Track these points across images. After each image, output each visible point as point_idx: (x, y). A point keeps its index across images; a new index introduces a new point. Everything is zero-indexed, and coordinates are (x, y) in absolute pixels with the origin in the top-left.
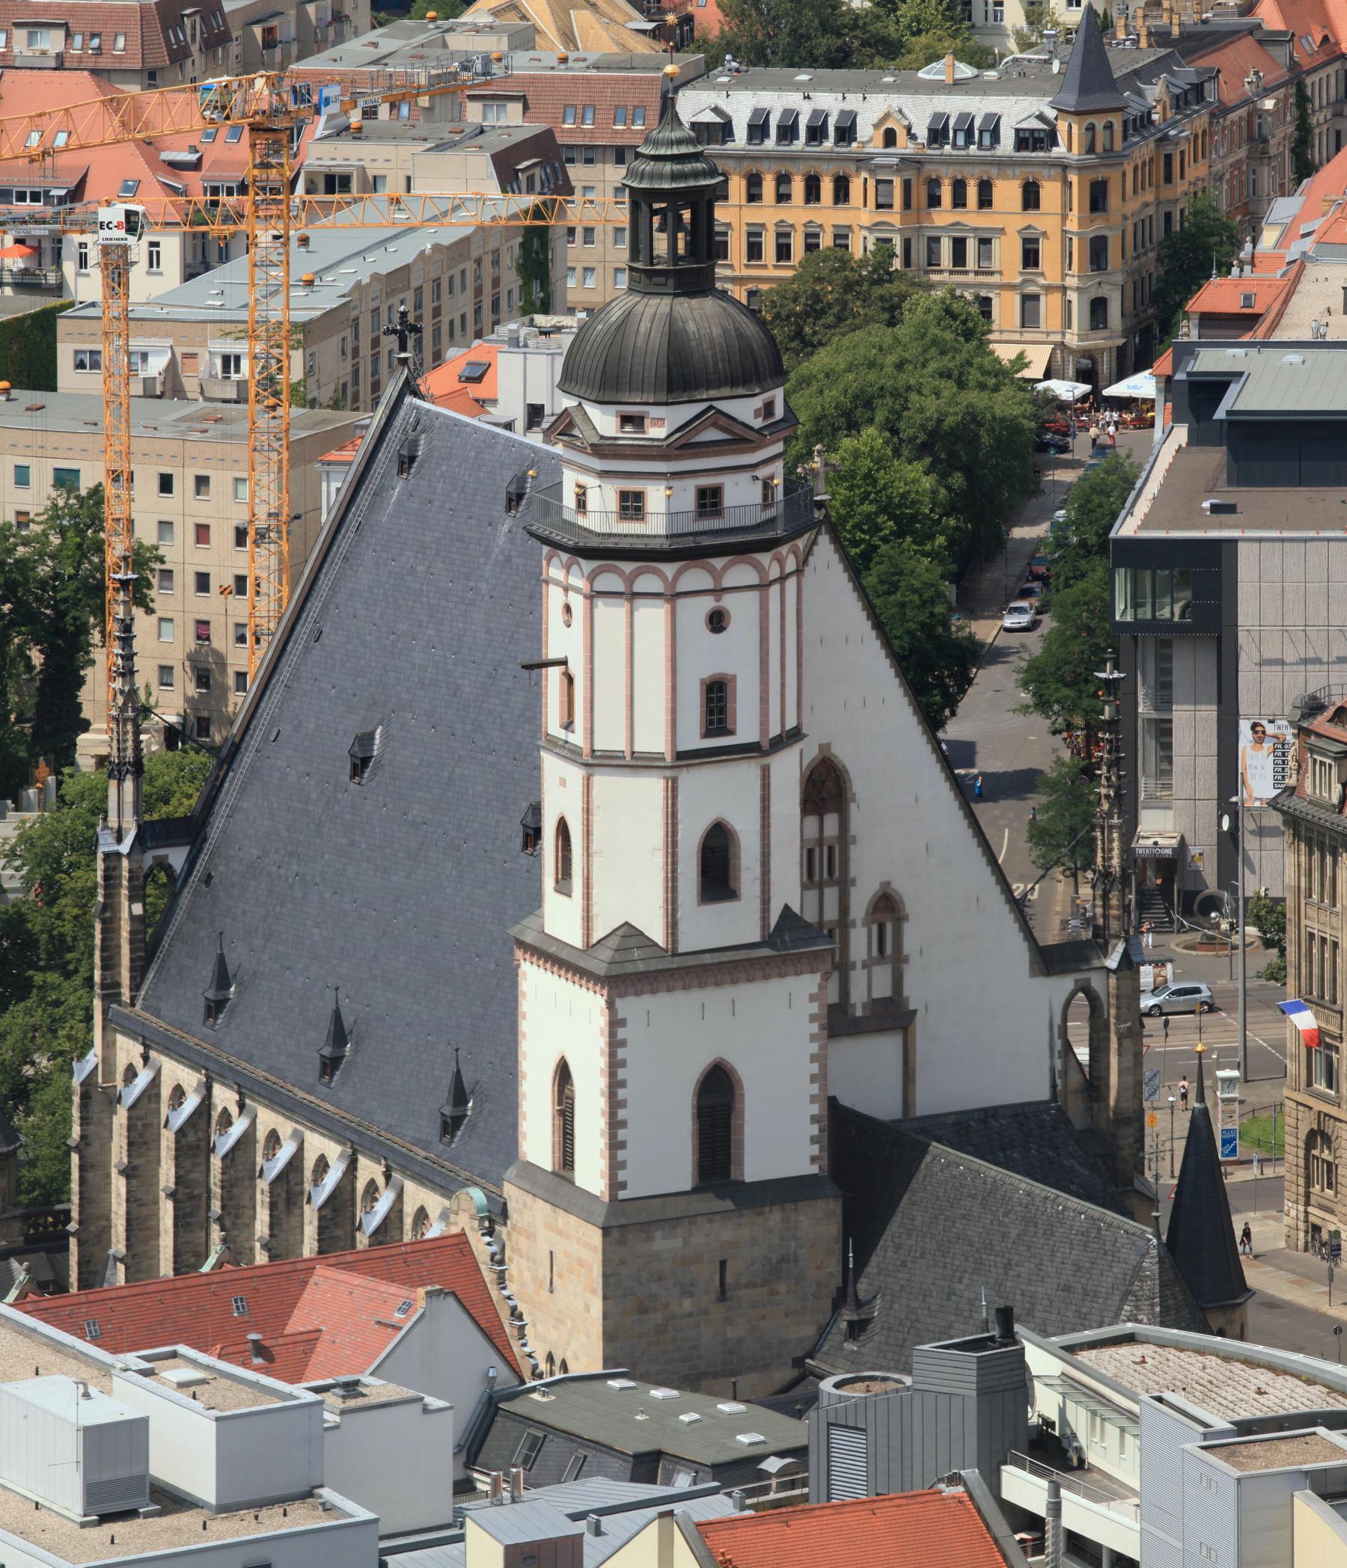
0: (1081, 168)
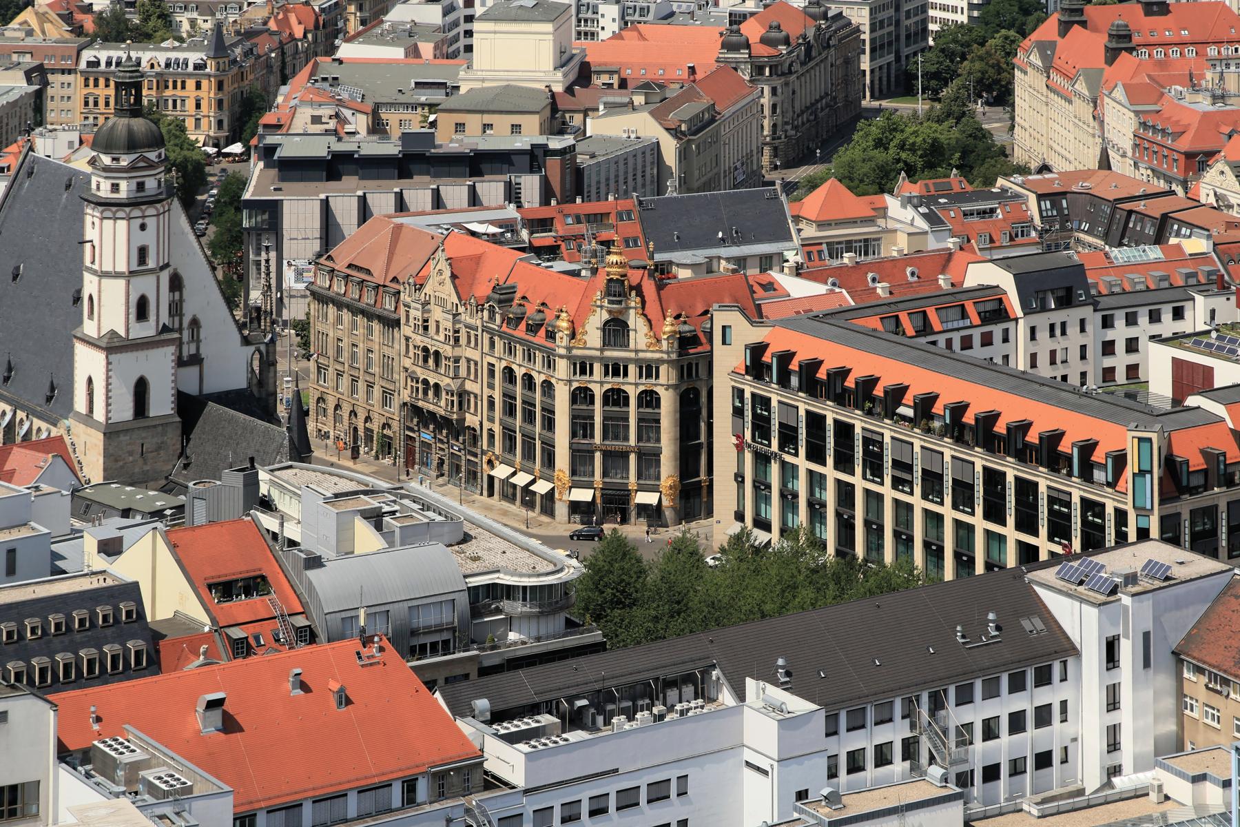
0: (215, 76)
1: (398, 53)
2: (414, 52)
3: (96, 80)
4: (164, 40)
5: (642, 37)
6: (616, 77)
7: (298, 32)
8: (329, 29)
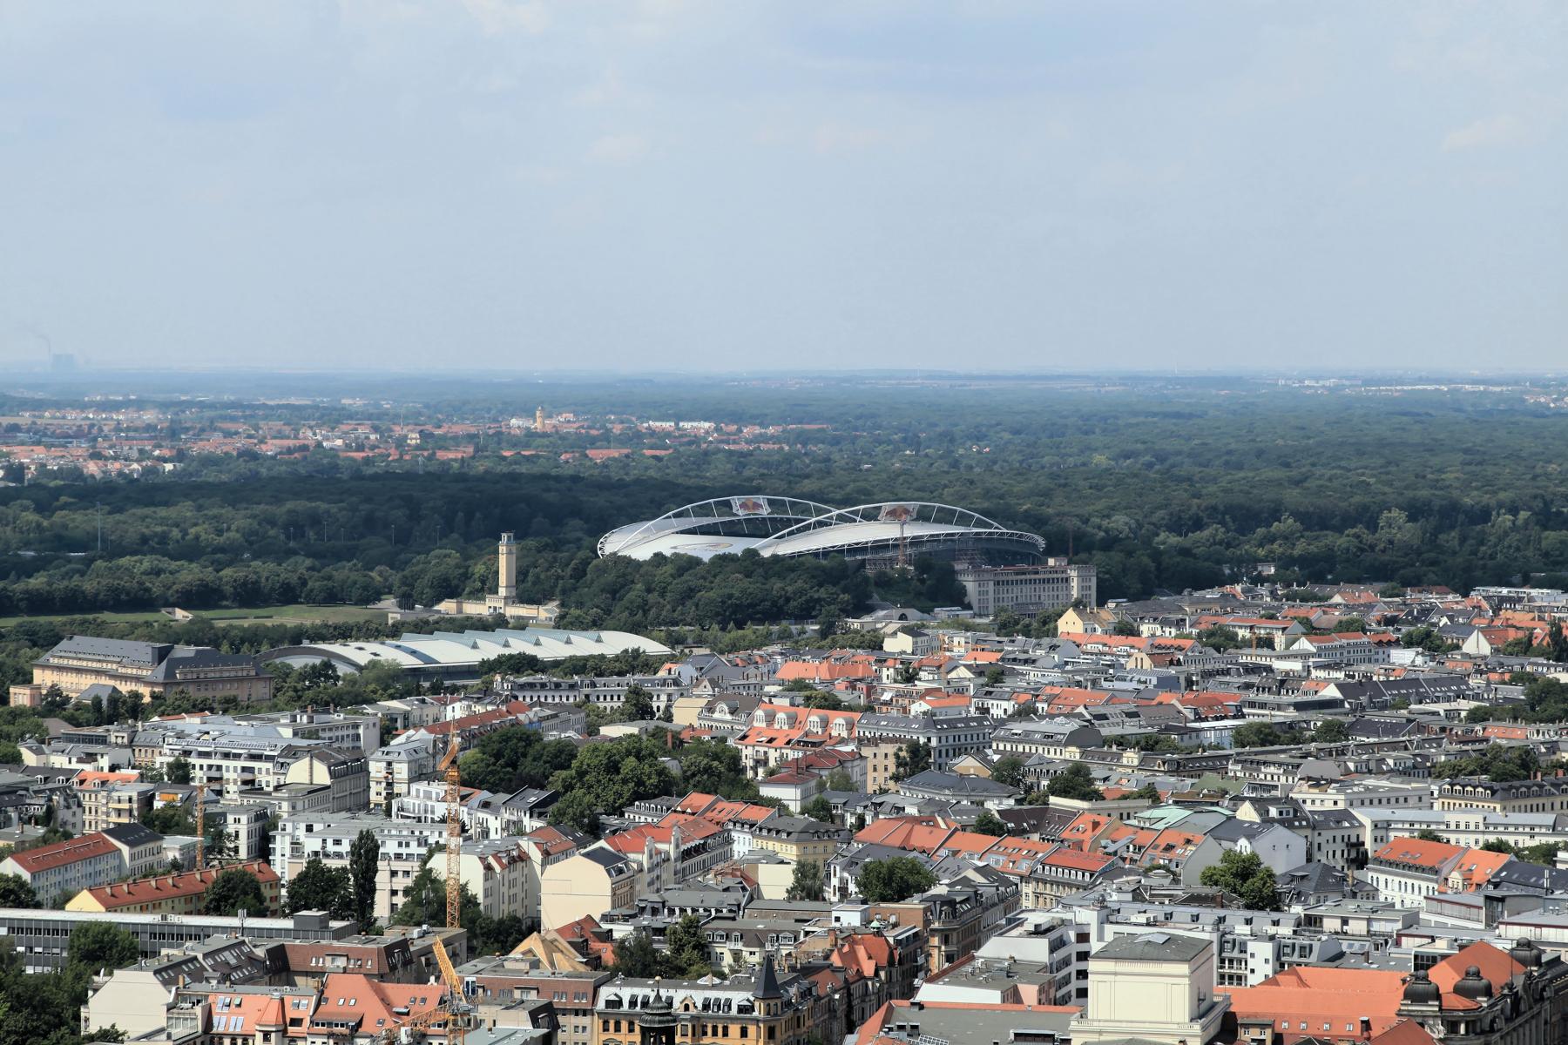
0: (764, 1021)
1: (993, 997)
2: (1013, 996)
3: (618, 1024)
4: (700, 976)
5: (1302, 982)
6: (1269, 1031)
7: (868, 968)
8: (906, 966)
